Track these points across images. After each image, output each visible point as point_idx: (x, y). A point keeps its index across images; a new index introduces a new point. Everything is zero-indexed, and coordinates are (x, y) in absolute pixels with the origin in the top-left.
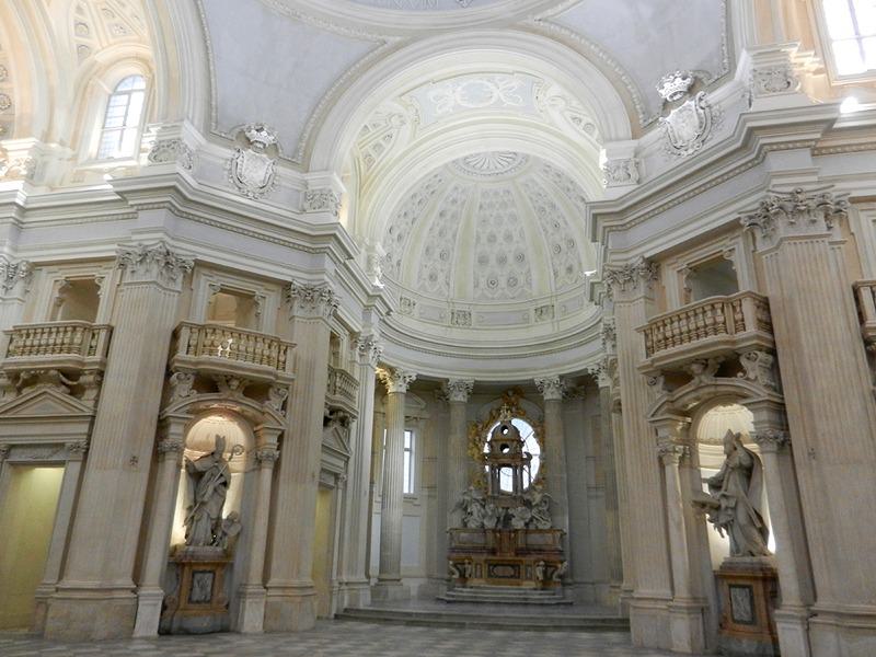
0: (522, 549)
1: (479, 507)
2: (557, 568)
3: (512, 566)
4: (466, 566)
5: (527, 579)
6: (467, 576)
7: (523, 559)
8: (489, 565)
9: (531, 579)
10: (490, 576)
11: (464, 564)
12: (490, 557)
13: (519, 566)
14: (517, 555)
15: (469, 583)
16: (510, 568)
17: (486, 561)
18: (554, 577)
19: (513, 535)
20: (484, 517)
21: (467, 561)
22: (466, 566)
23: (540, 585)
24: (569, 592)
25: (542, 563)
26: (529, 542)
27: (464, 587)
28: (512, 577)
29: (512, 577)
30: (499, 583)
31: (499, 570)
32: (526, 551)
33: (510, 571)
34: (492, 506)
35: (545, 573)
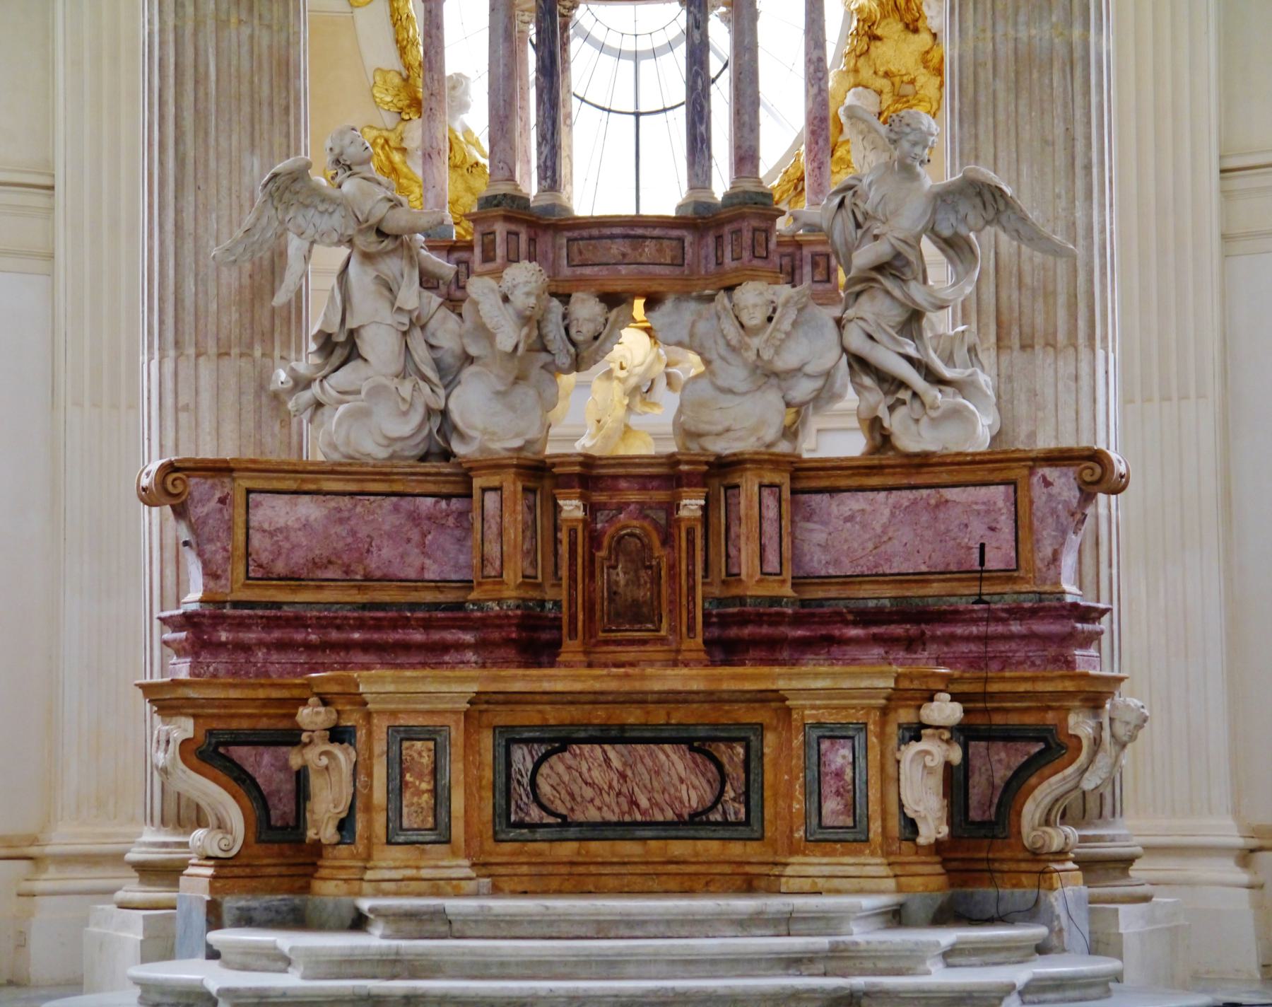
0: (768, 612)
1: (410, 295)
2: (1053, 749)
3: (699, 745)
4: (312, 756)
5: (823, 838)
6: (321, 826)
7: (780, 679)
8: (509, 738)
9: (852, 837)
10: (506, 822)
11: (292, 738)
12: (520, 680)
13: (749, 737)
14: (725, 650)
15: (329, 891)
16: (674, 760)
17: (477, 699)
18: (1031, 811)
19: (691, 506)
20: (449, 373)
21: (311, 716)
22: (312, 756)
23: (928, 883)
24: (1129, 920)
25: (946, 711)
26: (817, 562)
27: (298, 920)
28: (693, 823)
29: (693, 823)
30: (579, 881)
31: (586, 779)
32: (815, 622)
33: (677, 779)
34: (524, 278)
35: (955, 782)
